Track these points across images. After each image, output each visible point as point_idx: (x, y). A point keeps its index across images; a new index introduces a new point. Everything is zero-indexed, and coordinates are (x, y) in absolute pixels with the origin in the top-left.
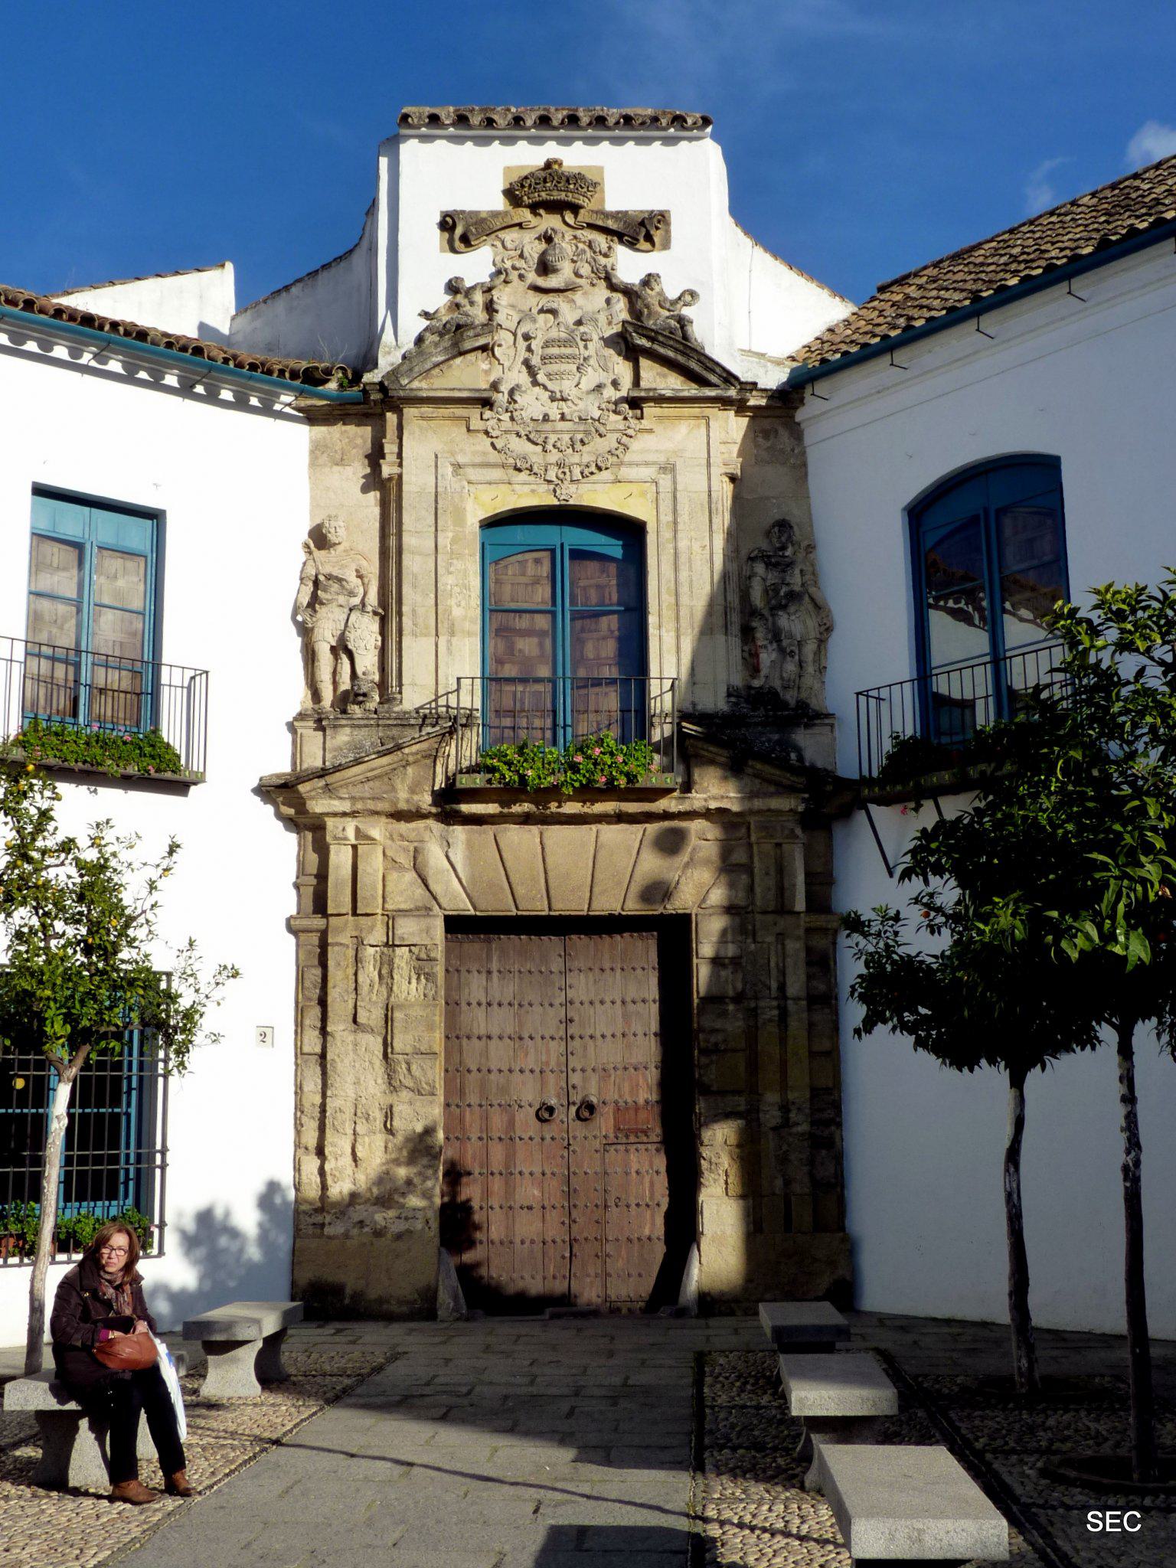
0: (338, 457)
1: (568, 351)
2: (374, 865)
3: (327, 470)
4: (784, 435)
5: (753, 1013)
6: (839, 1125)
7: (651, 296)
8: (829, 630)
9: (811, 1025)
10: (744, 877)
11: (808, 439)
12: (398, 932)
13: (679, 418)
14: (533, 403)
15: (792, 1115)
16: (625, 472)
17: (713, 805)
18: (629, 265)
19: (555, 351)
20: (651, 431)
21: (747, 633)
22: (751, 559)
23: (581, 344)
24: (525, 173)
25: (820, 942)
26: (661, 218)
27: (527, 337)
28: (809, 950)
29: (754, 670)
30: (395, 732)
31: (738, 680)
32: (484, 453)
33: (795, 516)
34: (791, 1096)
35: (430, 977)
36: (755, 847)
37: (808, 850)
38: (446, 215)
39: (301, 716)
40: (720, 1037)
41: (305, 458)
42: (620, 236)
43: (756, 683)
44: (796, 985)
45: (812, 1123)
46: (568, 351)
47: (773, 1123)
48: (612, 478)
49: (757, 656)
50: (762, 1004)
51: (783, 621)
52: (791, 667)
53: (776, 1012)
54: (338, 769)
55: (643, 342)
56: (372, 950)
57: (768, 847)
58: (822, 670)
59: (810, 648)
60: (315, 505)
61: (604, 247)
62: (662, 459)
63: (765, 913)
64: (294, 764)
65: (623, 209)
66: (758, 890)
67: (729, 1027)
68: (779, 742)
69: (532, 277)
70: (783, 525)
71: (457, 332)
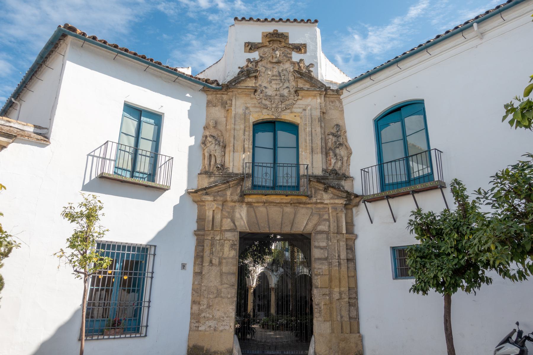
2: (218, 217)
4: (337, 102)
5: (330, 264)
6: (357, 299)
7: (301, 65)
8: (351, 154)
9: (348, 268)
10: (328, 223)
11: (344, 104)
12: (226, 236)
13: (309, 96)
15: (343, 295)
16: (294, 110)
17: (318, 201)
18: (296, 57)
19: (275, 78)
20: (301, 99)
21: (327, 154)
25: (350, 243)
26: (305, 46)
28: (347, 245)
29: (330, 164)
30: (227, 178)
31: (325, 167)
32: (255, 104)
33: (341, 123)
34: (342, 289)
35: (235, 249)
36: (331, 215)
37: (346, 215)
38: (246, 43)
40: (320, 271)
41: (205, 105)
42: (293, 49)
44: (343, 256)
45: (349, 298)
49: (330, 160)
50: (333, 261)
51: (337, 151)
52: (339, 163)
53: (337, 263)
56: (218, 241)
57: (335, 214)
59: (345, 159)
62: (304, 107)
63: (334, 233)
66: (332, 227)
67: (323, 267)
70: (337, 125)
71: (248, 72)
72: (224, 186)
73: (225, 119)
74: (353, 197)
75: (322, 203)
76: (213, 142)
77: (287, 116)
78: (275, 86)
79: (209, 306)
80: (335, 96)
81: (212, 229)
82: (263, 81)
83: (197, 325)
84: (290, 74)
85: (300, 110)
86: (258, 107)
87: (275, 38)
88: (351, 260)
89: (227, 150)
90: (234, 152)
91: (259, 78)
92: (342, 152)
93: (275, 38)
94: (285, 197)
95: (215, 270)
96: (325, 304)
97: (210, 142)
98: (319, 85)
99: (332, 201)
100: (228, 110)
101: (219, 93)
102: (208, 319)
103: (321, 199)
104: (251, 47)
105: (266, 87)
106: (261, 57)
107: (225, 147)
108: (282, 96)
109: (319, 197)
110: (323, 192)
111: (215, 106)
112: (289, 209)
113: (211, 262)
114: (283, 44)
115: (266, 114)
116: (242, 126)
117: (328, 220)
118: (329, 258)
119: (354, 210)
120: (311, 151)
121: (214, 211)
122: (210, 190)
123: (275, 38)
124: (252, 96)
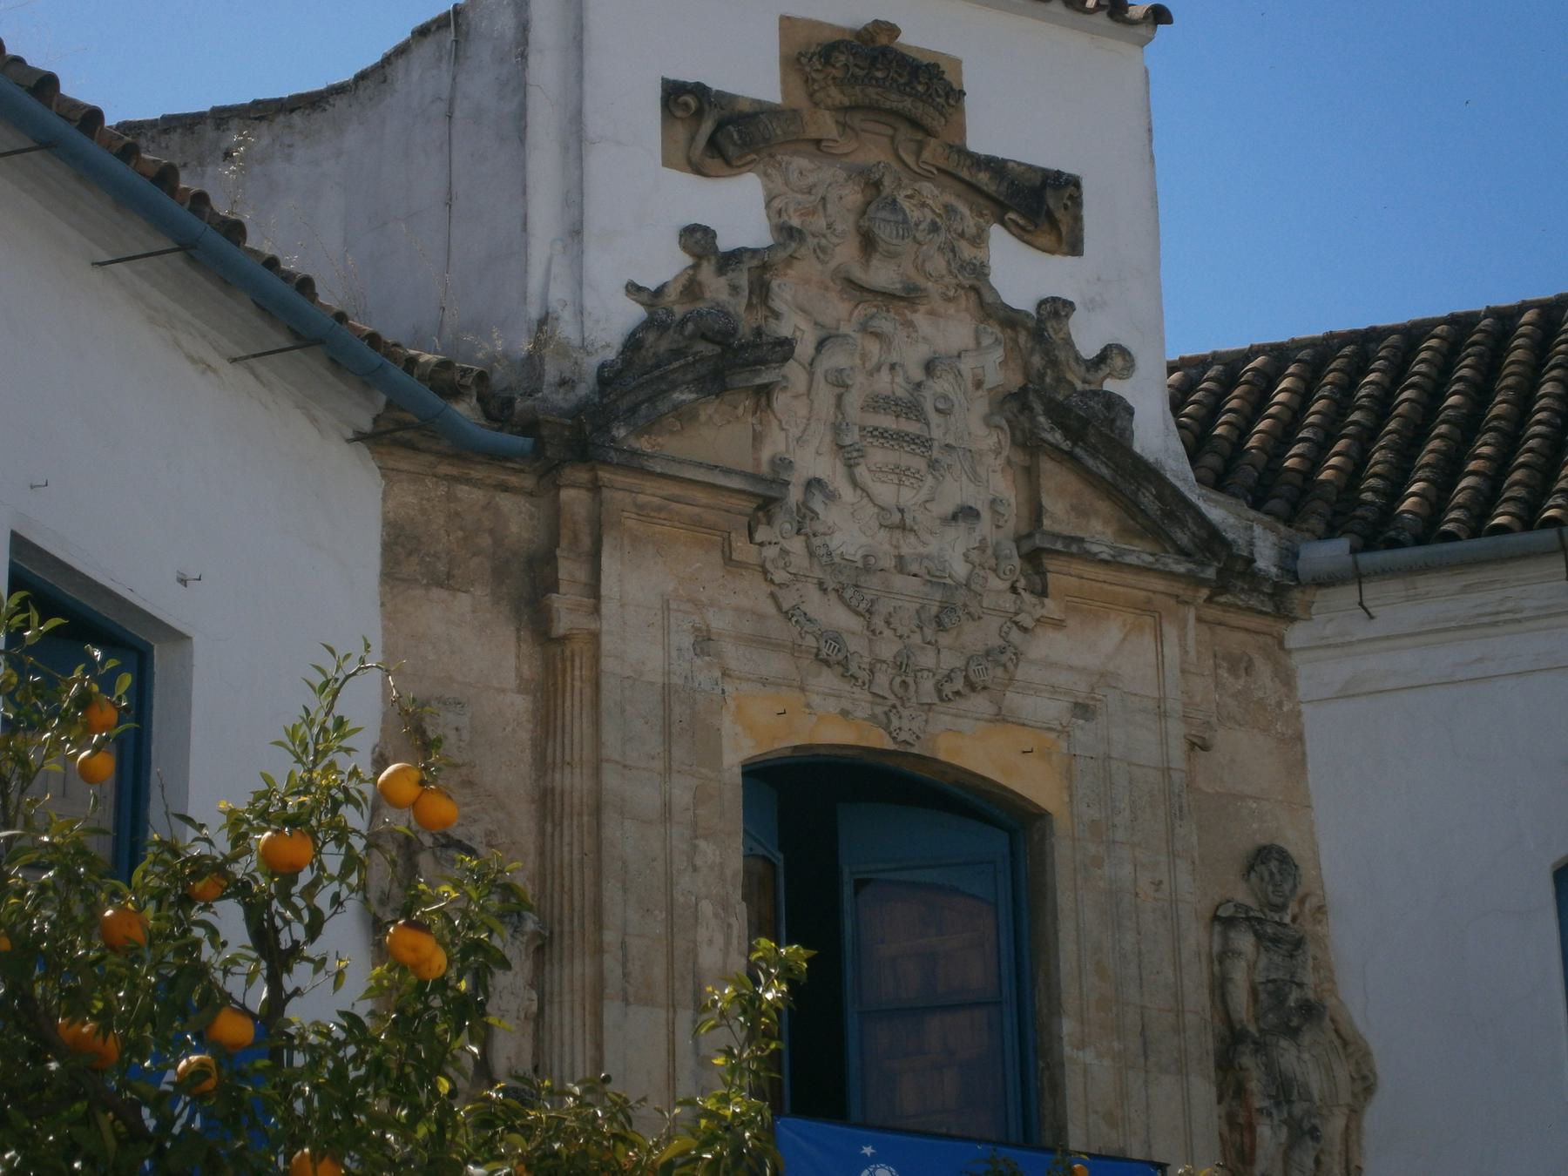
0: (441, 567)
1: (912, 427)
3: (418, 592)
4: (1263, 669)
11: (1303, 687)
14: (849, 531)
18: (1019, 271)
19: (887, 422)
20: (1058, 625)
22: (1228, 923)
23: (934, 418)
24: (837, 38)
27: (840, 383)
32: (761, 617)
46: (912, 427)
48: (992, 710)
49: (1251, 1128)
55: (1057, 437)
59: (1334, 1126)
61: (971, 230)
62: (1082, 688)
65: (1000, 155)
71: (706, 346)
73: (520, 705)
77: (970, 745)
78: (885, 492)
82: (797, 433)
84: (981, 406)
86: (776, 646)
91: (780, 401)
92: (1301, 1060)
101: (478, 473)
105: (814, 484)
106: (788, 233)
108: (935, 579)
111: (445, 581)
114: (933, 152)
115: (832, 706)
116: (681, 795)
123: (894, 101)
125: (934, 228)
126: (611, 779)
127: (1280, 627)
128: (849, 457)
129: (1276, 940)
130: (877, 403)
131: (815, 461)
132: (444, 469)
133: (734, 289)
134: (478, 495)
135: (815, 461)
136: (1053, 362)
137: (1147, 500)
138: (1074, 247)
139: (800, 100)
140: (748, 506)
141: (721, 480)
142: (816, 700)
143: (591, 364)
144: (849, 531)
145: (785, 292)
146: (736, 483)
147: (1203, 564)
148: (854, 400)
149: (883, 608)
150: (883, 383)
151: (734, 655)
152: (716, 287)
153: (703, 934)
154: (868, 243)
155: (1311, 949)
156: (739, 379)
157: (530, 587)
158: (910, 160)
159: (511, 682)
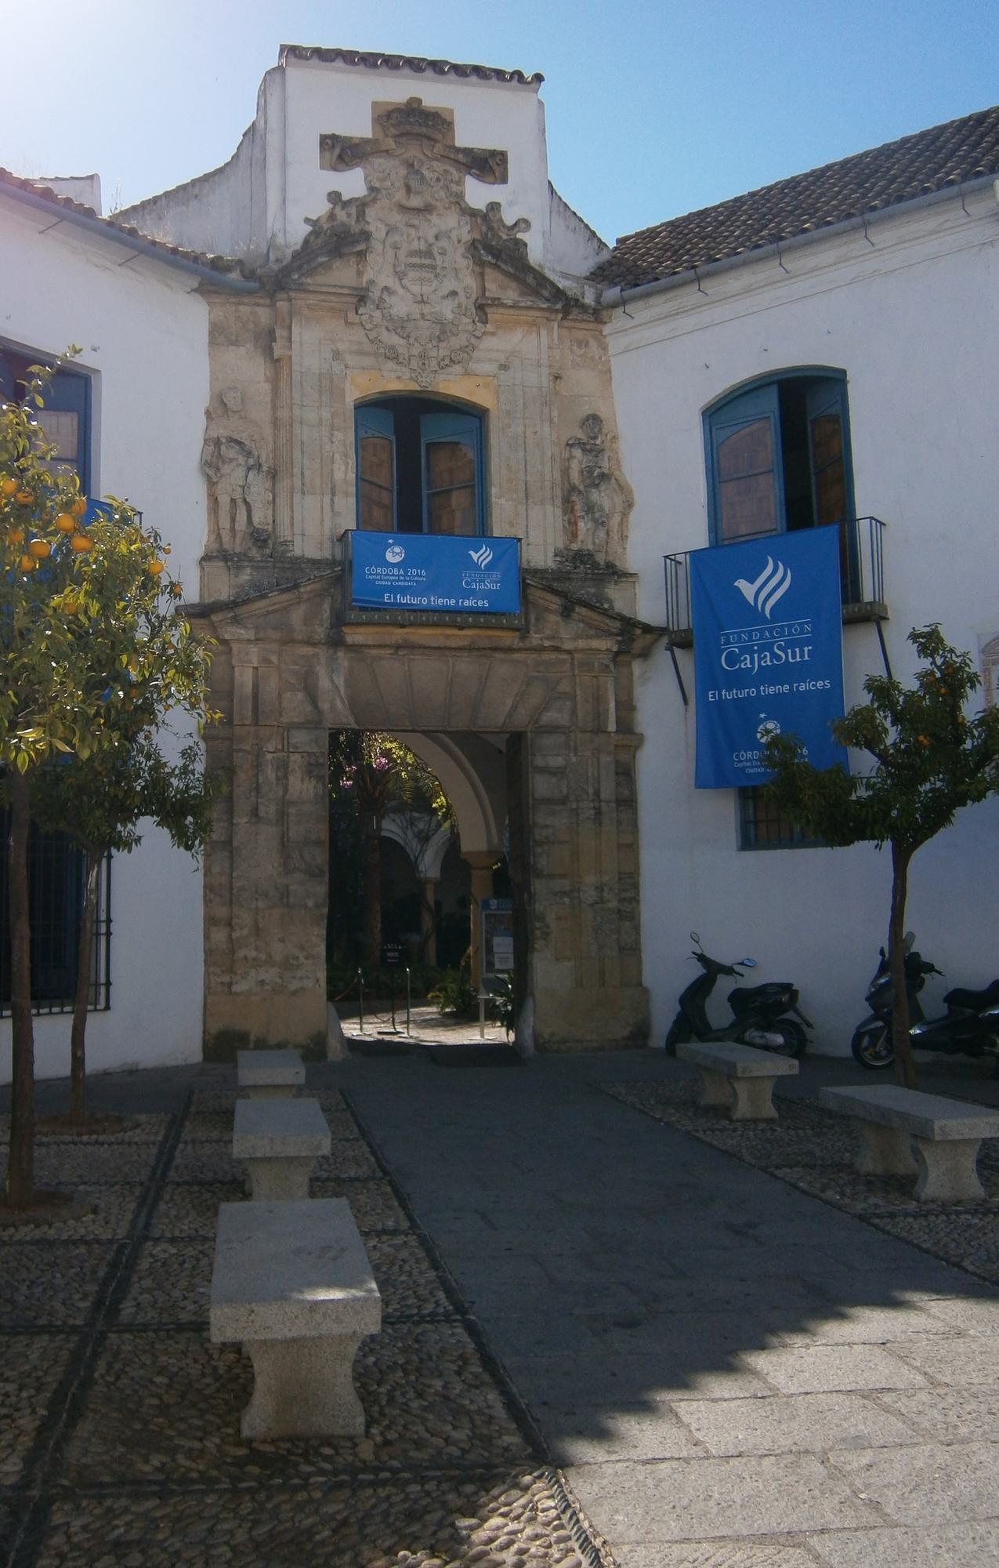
1: (428, 262)
2: (271, 686)
5: (576, 812)
6: (638, 902)
8: (629, 505)
9: (619, 823)
12: (293, 741)
14: (401, 306)
15: (605, 894)
17: (547, 643)
18: (477, 193)
19: (416, 260)
20: (493, 334)
22: (571, 446)
26: (501, 157)
27: (396, 247)
28: (617, 762)
29: (574, 535)
31: (561, 546)
32: (360, 343)
33: (603, 413)
34: (605, 879)
35: (320, 778)
38: (324, 139)
39: (206, 558)
40: (550, 830)
41: (206, 338)
43: (575, 547)
44: (607, 793)
46: (428, 262)
47: (590, 901)
50: (581, 805)
51: (595, 495)
52: (602, 534)
53: (592, 812)
54: (246, 602)
56: (269, 756)
58: (624, 538)
59: (616, 520)
60: (214, 378)
63: (584, 731)
64: (201, 596)
66: (580, 714)
68: (594, 595)
69: (400, 196)
71: (338, 239)
72: (284, 597)
73: (267, 386)
74: (638, 632)
75: (557, 649)
76: (241, 460)
77: (454, 386)
78: (416, 289)
79: (257, 930)
80: (590, 326)
81: (256, 722)
82: (379, 271)
83: (226, 979)
84: (461, 250)
85: (491, 368)
87: (415, 127)
88: (628, 803)
89: (283, 485)
90: (303, 493)
91: (370, 258)
92: (603, 498)
93: (415, 127)
94: (456, 632)
95: (268, 834)
96: (559, 918)
97: (231, 460)
98: (546, 293)
99: (581, 644)
100: (278, 360)
101: (246, 300)
102: (256, 963)
103: (553, 638)
104: (340, 151)
105: (386, 288)
106: (372, 189)
107: (273, 475)
108: (439, 321)
109: (548, 632)
110: (559, 619)
111: (236, 343)
112: (465, 666)
113: (255, 813)
115: (393, 375)
116: (326, 414)
117: (572, 697)
118: (572, 798)
119: (637, 667)
120: (522, 495)
121: (256, 668)
122: (245, 608)
123: (417, 129)
124: (352, 317)
125: (438, 180)
126: (297, 411)
127: (601, 326)
128: (400, 276)
129: (591, 451)
130: (413, 253)
131: (386, 279)
132: (232, 300)
133: (349, 215)
134: (249, 309)
135: (386, 279)
136: (491, 228)
137: (530, 279)
138: (504, 180)
139: (380, 136)
140: (355, 300)
141: (339, 291)
142: (386, 374)
143: (289, 252)
144: (401, 306)
145: (371, 213)
146: (346, 291)
147: (555, 303)
148: (402, 253)
149: (413, 336)
150: (415, 245)
151: (350, 360)
152: (341, 215)
153: (336, 466)
154: (409, 189)
155: (607, 454)
156: (346, 250)
157: (266, 341)
158: (429, 153)
159: (262, 378)
